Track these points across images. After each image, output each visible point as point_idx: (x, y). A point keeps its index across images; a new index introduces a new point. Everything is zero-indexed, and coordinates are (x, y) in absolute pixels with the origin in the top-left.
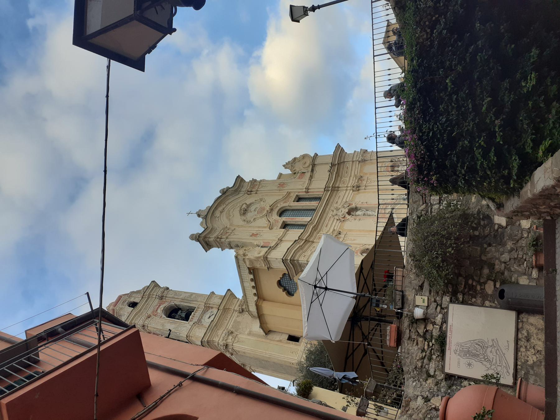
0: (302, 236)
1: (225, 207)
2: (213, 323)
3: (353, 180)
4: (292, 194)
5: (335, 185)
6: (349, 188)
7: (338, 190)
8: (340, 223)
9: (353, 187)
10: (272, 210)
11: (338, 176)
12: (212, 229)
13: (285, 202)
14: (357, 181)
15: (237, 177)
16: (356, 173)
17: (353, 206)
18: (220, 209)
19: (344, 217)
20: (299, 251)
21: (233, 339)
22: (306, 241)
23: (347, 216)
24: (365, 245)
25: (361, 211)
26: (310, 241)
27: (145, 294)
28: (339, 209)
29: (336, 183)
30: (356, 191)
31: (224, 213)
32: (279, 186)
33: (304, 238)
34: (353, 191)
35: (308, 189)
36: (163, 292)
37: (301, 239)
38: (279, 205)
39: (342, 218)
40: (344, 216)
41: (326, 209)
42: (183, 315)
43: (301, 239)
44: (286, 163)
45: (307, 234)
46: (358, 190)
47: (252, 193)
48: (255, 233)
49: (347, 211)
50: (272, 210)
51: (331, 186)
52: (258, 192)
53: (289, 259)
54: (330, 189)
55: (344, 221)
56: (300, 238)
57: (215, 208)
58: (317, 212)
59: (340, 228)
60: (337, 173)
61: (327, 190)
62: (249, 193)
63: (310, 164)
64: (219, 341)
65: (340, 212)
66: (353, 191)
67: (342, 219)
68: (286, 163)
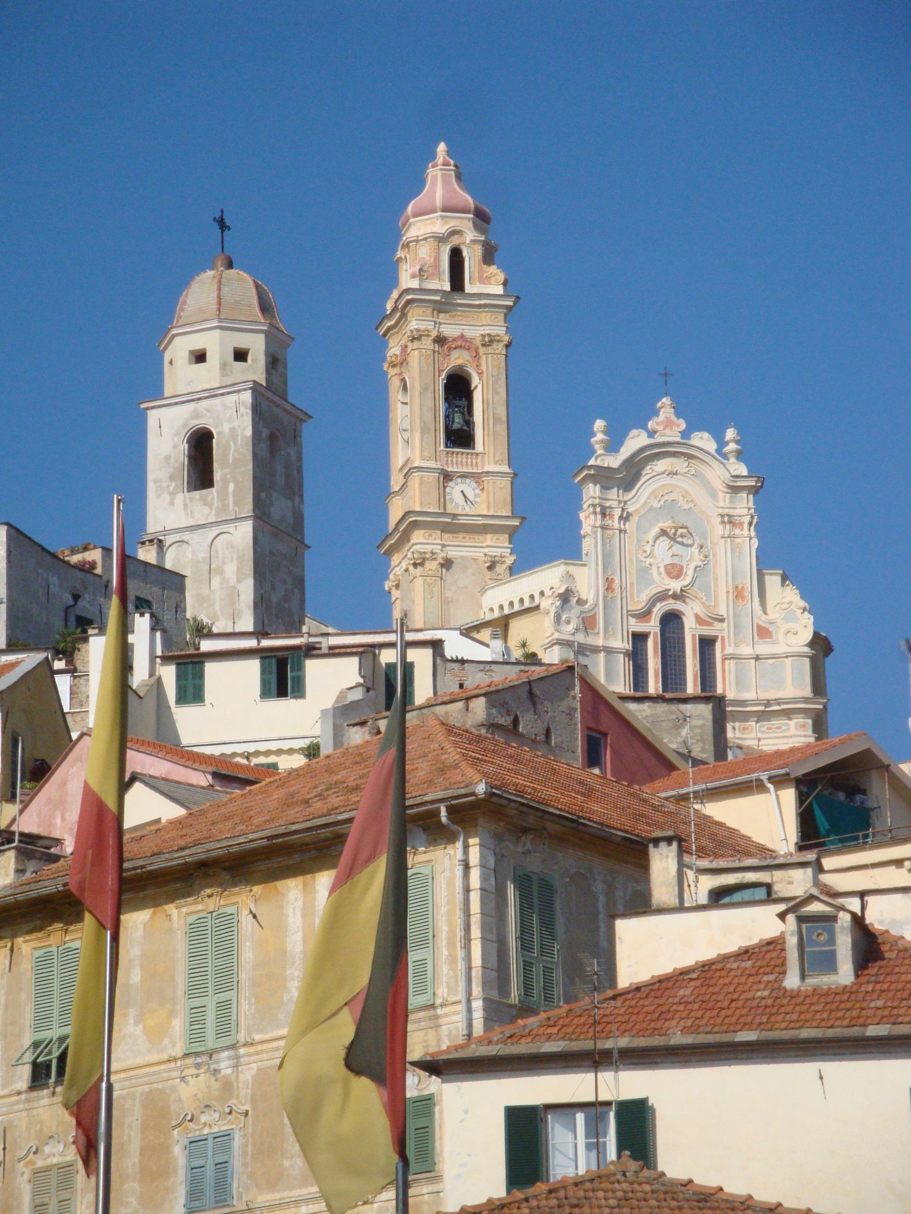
4: (717, 625)
10: (675, 596)
13: (697, 616)
32: (740, 587)
38: (689, 607)
50: (675, 596)
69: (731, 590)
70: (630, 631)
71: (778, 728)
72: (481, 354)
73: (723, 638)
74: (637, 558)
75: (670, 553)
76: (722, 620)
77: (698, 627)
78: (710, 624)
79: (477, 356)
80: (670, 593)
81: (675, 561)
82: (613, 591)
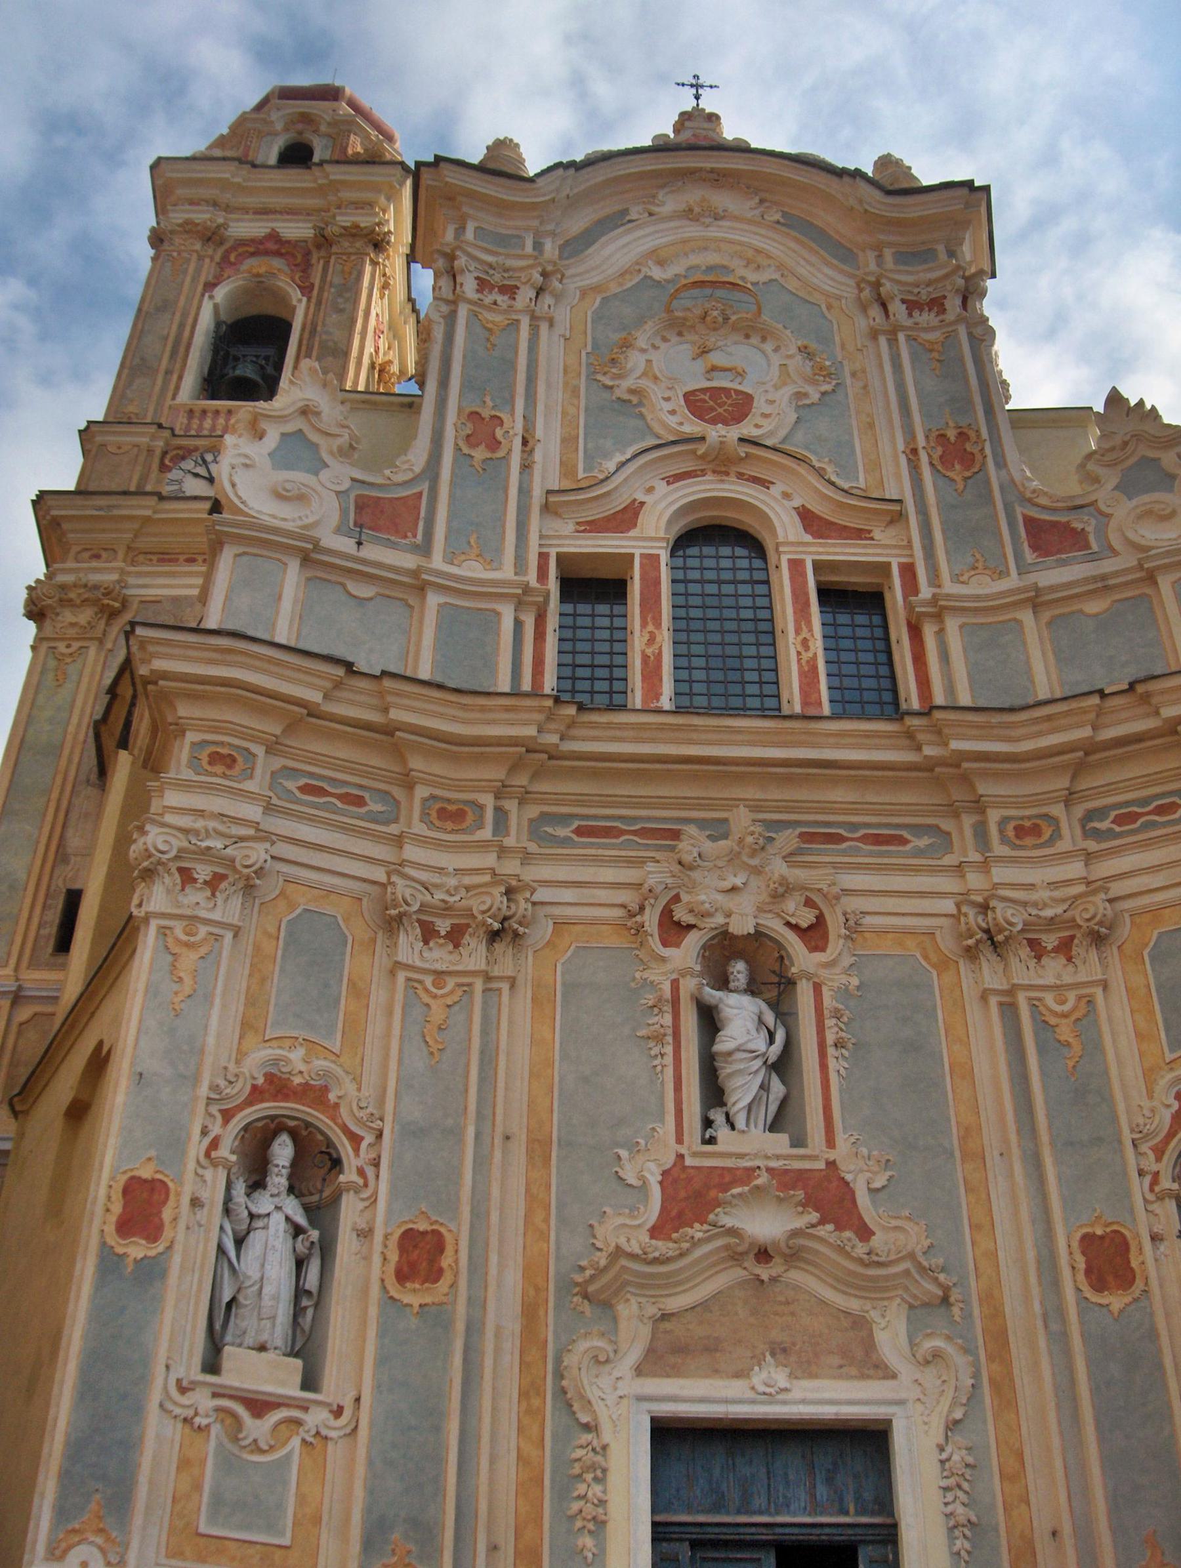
0: (398, 694)
1: (736, 218)
2: (152, 501)
3: (1053, 885)
5: (984, 774)
6: (975, 880)
7: (956, 815)
8: (620, 912)
9: (984, 908)
11: (1079, 770)
12: (534, 206)
13: (807, 517)
14: (1048, 913)
15: (969, 185)
16: (1117, 889)
17: (801, 957)
18: (723, 200)
19: (678, 924)
20: (262, 711)
21: (72, 632)
22: (389, 730)
23: (693, 942)
24: (380, 1135)
25: (770, 1018)
26: (398, 752)
27: (328, 168)
28: (757, 871)
29: (997, 776)
30: (960, 937)
31: (692, 231)
32: (952, 434)
33: (394, 714)
34: (956, 917)
35: (938, 617)
36: (354, 235)
37: (381, 694)
38: (776, 490)
39: (667, 913)
40: (691, 920)
41: (740, 778)
42: (246, 370)
43: (381, 694)
44: (1141, 403)
45: (454, 719)
46: (971, 954)
47: (875, 311)
48: (499, 433)
49: (742, 926)
51: (955, 745)
52: (883, 340)
53: (159, 664)
54: (928, 751)
55: (639, 929)
56: (387, 683)
57: (712, 171)
58: (678, 728)
59: (560, 925)
60: (1090, 748)
61: (910, 735)
62: (867, 293)
63: (1147, 549)
64: (64, 571)
65: (727, 885)
66: (956, 917)
67: (651, 919)
68: (1141, 403)
69: (921, 441)
70: (553, 552)
71: (1160, 811)
72: (314, 261)
73: (908, 571)
74: (591, 379)
75: (700, 366)
76: (897, 518)
77: (808, 538)
78: (860, 534)
79: (305, 267)
80: (702, 449)
81: (722, 381)
82: (494, 444)
